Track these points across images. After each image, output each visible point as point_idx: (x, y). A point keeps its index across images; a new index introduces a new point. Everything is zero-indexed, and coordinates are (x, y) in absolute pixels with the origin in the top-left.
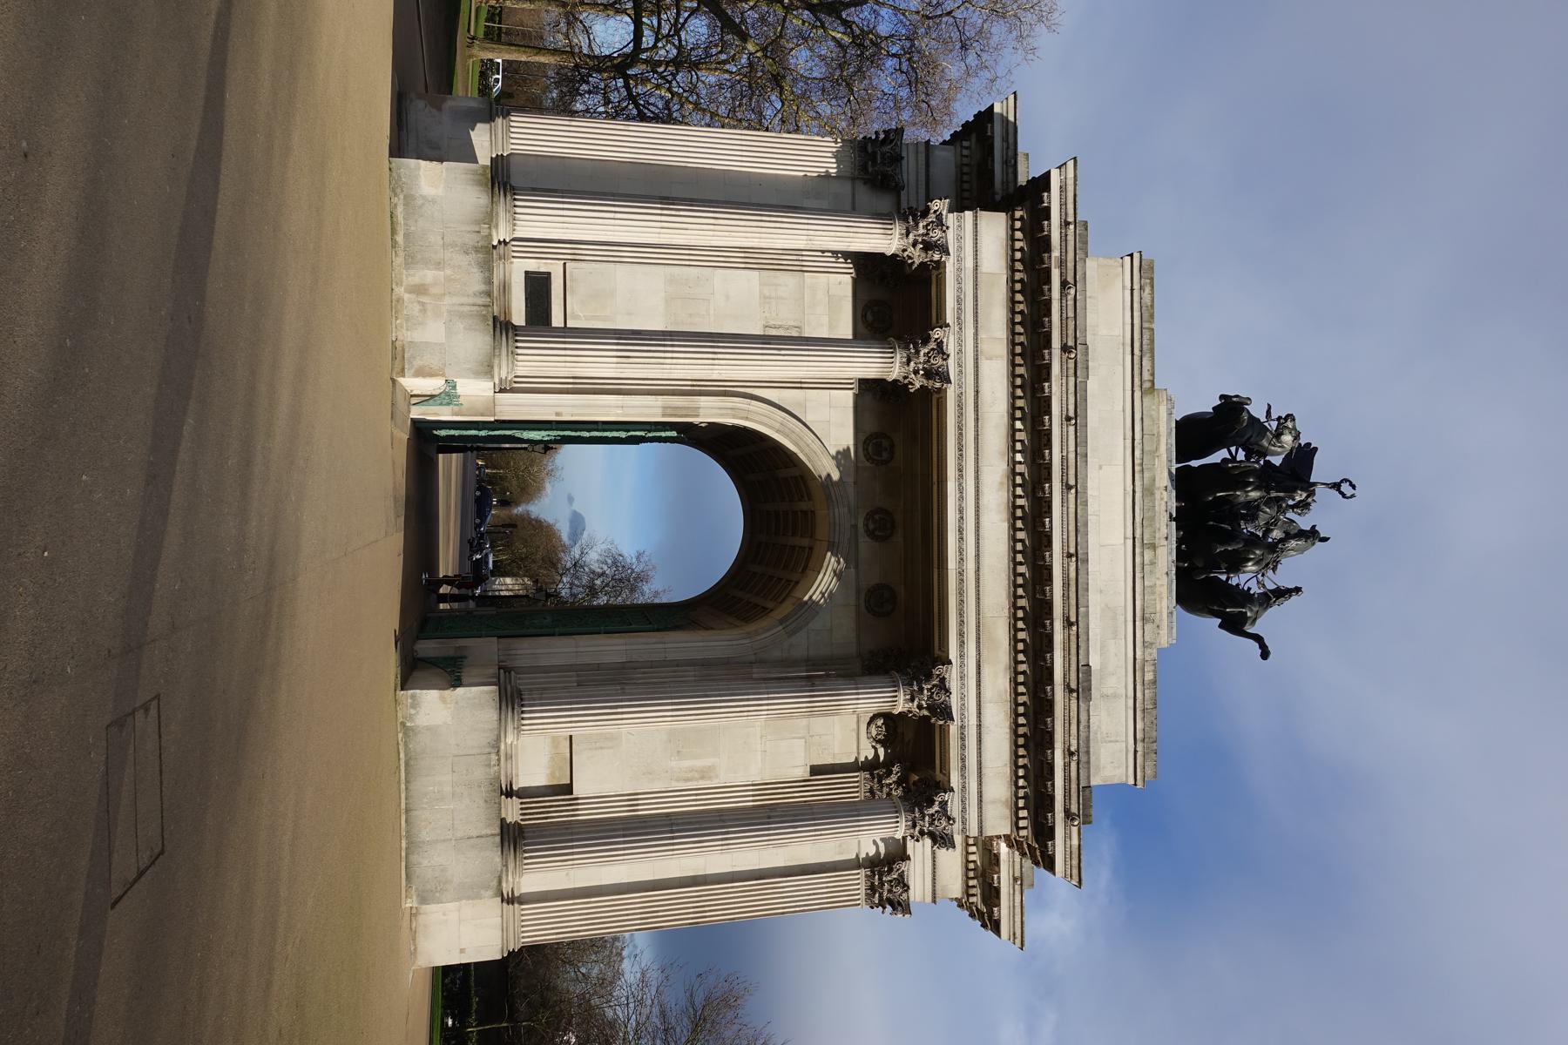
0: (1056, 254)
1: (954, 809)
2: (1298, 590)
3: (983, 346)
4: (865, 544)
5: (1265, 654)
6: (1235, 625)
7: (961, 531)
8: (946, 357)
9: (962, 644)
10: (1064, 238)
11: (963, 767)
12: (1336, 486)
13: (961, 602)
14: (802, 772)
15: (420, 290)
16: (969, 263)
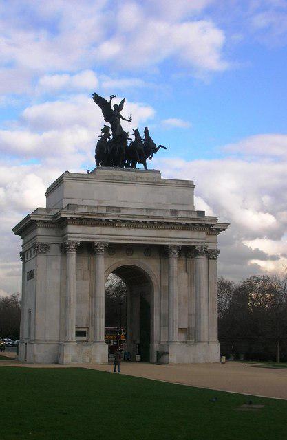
0: (80, 216)
1: (199, 245)
2: (146, 128)
3: (99, 232)
4: (134, 256)
5: (165, 148)
6: (156, 150)
7: (139, 240)
8: (101, 243)
9: (164, 241)
10: (78, 214)
11: (192, 242)
12: (111, 99)
13: (155, 241)
14: (186, 275)
15: (90, 359)
16: (80, 235)
